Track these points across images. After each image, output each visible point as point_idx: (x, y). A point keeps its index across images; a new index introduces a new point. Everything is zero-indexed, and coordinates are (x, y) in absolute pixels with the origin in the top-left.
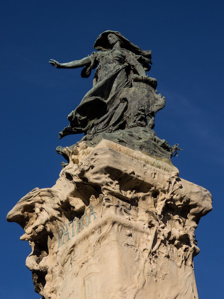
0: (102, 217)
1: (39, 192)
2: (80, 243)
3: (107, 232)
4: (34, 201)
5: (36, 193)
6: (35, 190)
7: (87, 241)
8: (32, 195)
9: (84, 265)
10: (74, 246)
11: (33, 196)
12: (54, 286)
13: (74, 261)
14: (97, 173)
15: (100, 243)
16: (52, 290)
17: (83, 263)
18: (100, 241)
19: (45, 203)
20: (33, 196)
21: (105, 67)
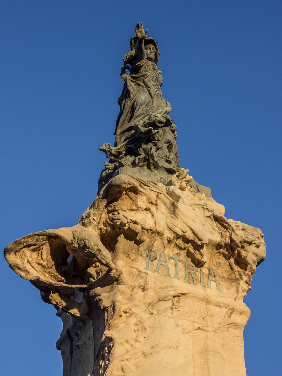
0: (235, 300)
1: (159, 192)
2: (193, 299)
3: (243, 325)
4: (146, 193)
5: (155, 188)
6: (156, 184)
7: (204, 305)
8: (151, 186)
9: (199, 330)
10: (183, 294)
11: (150, 187)
12: (134, 310)
13: (176, 310)
14: (257, 255)
15: (228, 328)
16: (126, 311)
17: (199, 328)
18: (230, 325)
19: (157, 209)
20: (150, 187)
21: (157, 84)
